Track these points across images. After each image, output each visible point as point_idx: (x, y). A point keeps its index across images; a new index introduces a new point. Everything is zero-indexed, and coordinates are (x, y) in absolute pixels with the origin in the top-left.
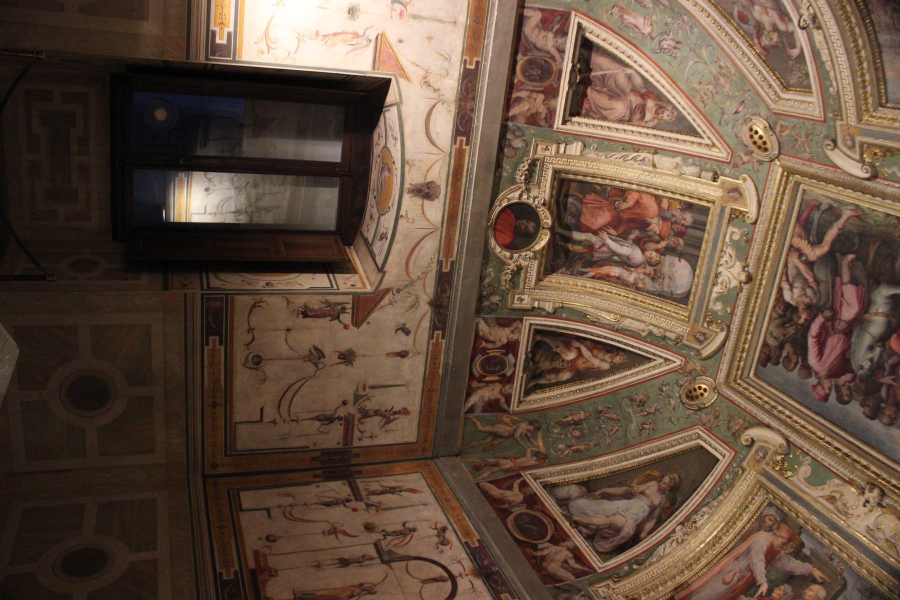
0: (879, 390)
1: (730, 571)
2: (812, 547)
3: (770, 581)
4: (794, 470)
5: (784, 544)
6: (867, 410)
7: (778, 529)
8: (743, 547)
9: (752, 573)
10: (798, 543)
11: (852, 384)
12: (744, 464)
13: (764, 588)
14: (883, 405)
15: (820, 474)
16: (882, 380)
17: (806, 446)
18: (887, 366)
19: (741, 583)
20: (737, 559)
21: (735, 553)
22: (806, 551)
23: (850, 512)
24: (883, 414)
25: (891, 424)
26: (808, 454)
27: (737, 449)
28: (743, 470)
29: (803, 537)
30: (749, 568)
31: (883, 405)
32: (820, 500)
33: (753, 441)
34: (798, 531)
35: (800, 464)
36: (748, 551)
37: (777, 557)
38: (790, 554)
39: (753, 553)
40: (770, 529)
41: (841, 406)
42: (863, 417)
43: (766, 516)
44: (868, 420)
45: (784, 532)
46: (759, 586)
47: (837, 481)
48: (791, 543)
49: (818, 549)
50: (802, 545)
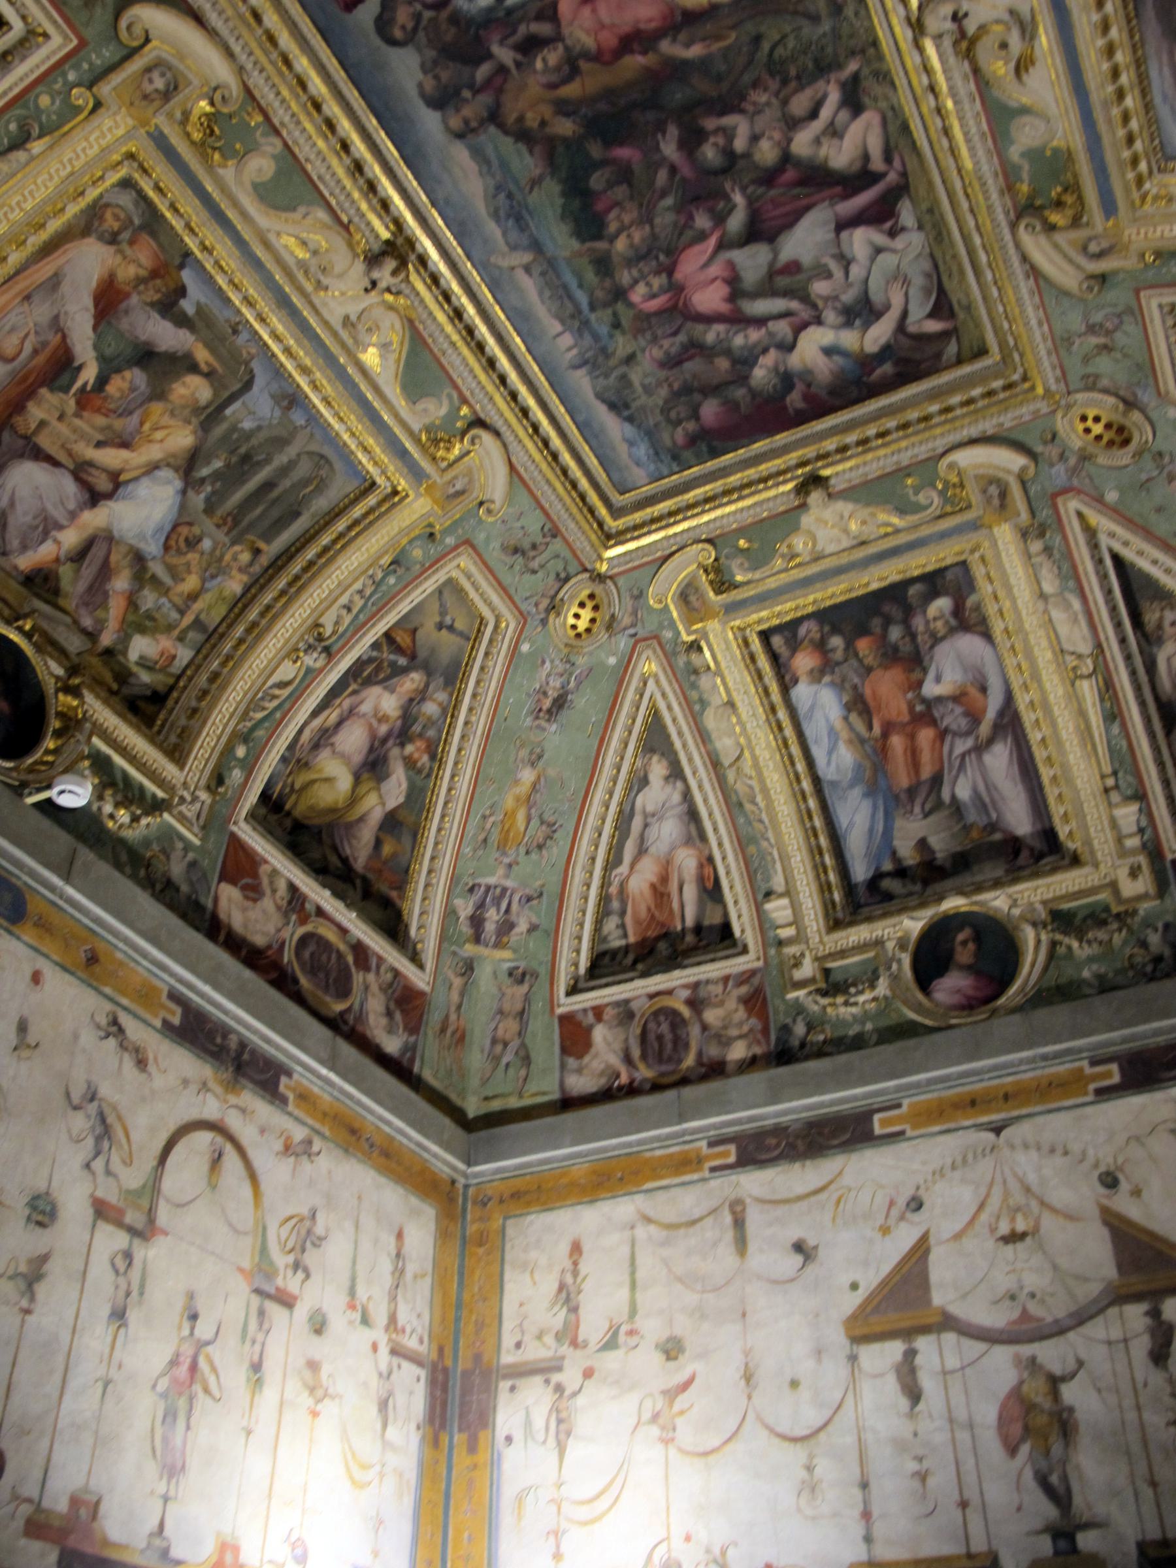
0: (477, 61)
1: (13, 329)
2: (203, 300)
3: (102, 359)
4: (228, 153)
5: (140, 281)
6: (430, 85)
7: (132, 242)
8: (45, 270)
9: (64, 337)
10: (172, 286)
11: (428, 14)
12: (105, 89)
13: (89, 374)
14: (466, 94)
15: (292, 186)
16: (496, 49)
17: (279, 116)
18: (522, 30)
19: (41, 359)
20: (27, 298)
21: (22, 284)
22: (187, 306)
23: (325, 281)
24: (458, 110)
25: (460, 136)
26: (277, 133)
27: (89, 33)
28: (98, 105)
29: (187, 276)
30: (56, 324)
31: (466, 94)
32: (272, 237)
33: (147, 40)
34: (177, 261)
35: (251, 149)
36: (54, 283)
37: (123, 306)
38: (152, 305)
39: (65, 288)
40: (112, 239)
41: (377, 41)
42: (413, 92)
43: (107, 205)
44: (420, 105)
45: (144, 255)
46: (80, 368)
47: (322, 214)
48: (158, 282)
49: (215, 307)
50: (182, 291)
